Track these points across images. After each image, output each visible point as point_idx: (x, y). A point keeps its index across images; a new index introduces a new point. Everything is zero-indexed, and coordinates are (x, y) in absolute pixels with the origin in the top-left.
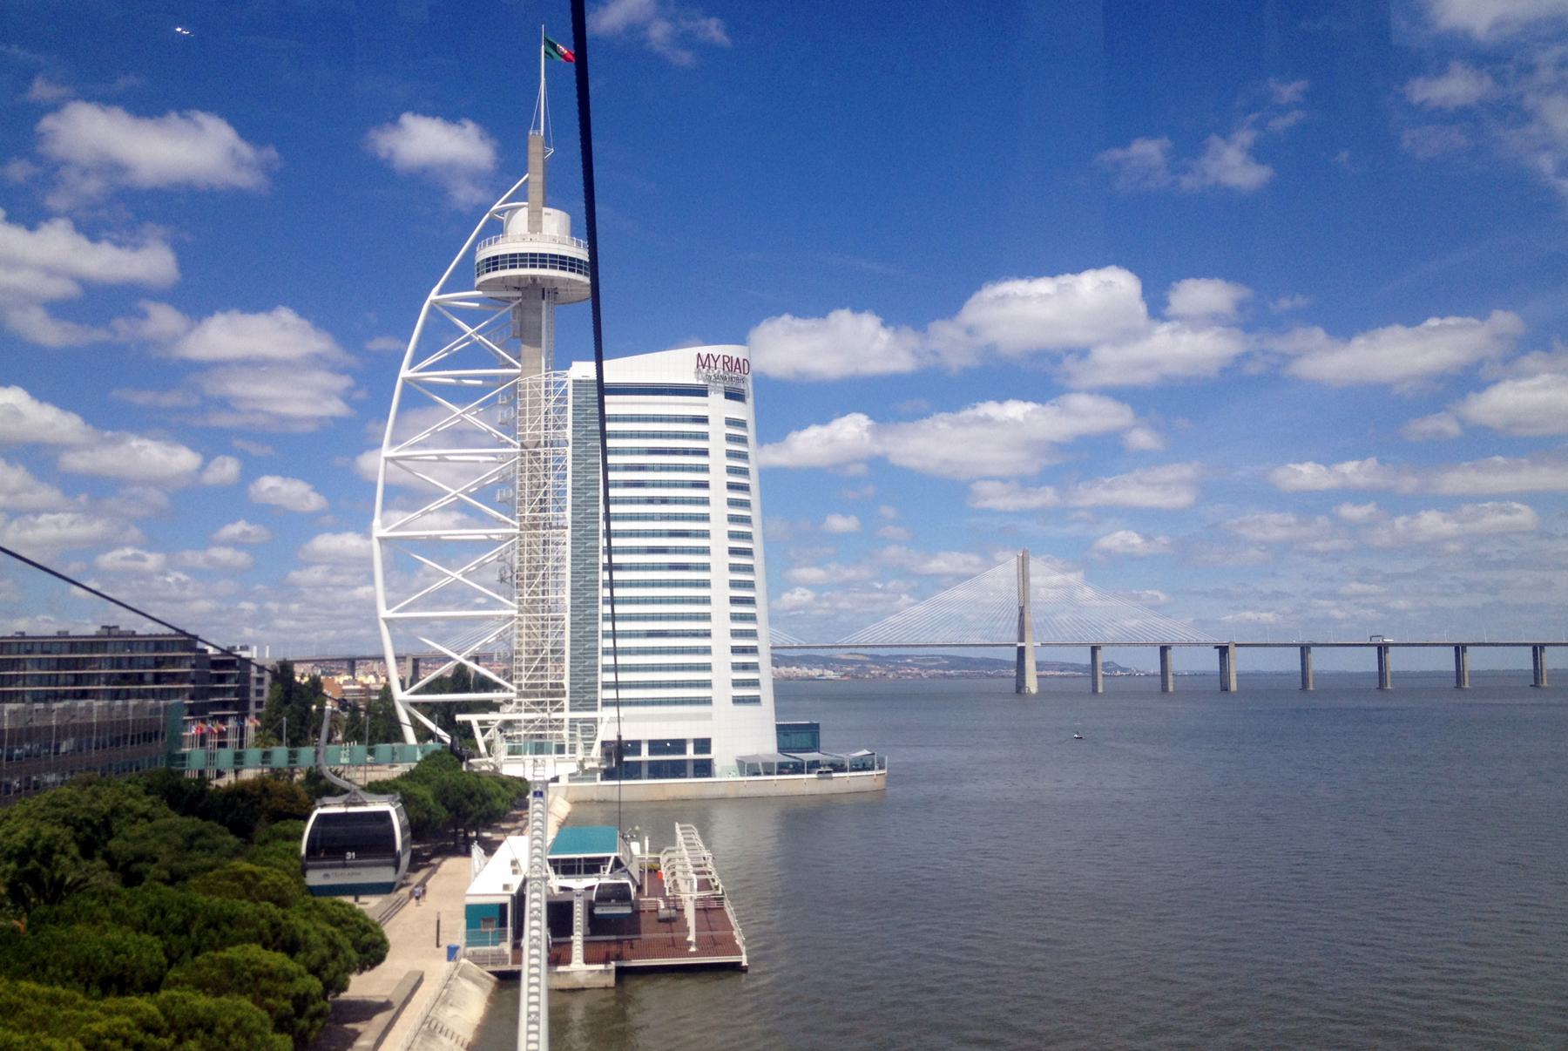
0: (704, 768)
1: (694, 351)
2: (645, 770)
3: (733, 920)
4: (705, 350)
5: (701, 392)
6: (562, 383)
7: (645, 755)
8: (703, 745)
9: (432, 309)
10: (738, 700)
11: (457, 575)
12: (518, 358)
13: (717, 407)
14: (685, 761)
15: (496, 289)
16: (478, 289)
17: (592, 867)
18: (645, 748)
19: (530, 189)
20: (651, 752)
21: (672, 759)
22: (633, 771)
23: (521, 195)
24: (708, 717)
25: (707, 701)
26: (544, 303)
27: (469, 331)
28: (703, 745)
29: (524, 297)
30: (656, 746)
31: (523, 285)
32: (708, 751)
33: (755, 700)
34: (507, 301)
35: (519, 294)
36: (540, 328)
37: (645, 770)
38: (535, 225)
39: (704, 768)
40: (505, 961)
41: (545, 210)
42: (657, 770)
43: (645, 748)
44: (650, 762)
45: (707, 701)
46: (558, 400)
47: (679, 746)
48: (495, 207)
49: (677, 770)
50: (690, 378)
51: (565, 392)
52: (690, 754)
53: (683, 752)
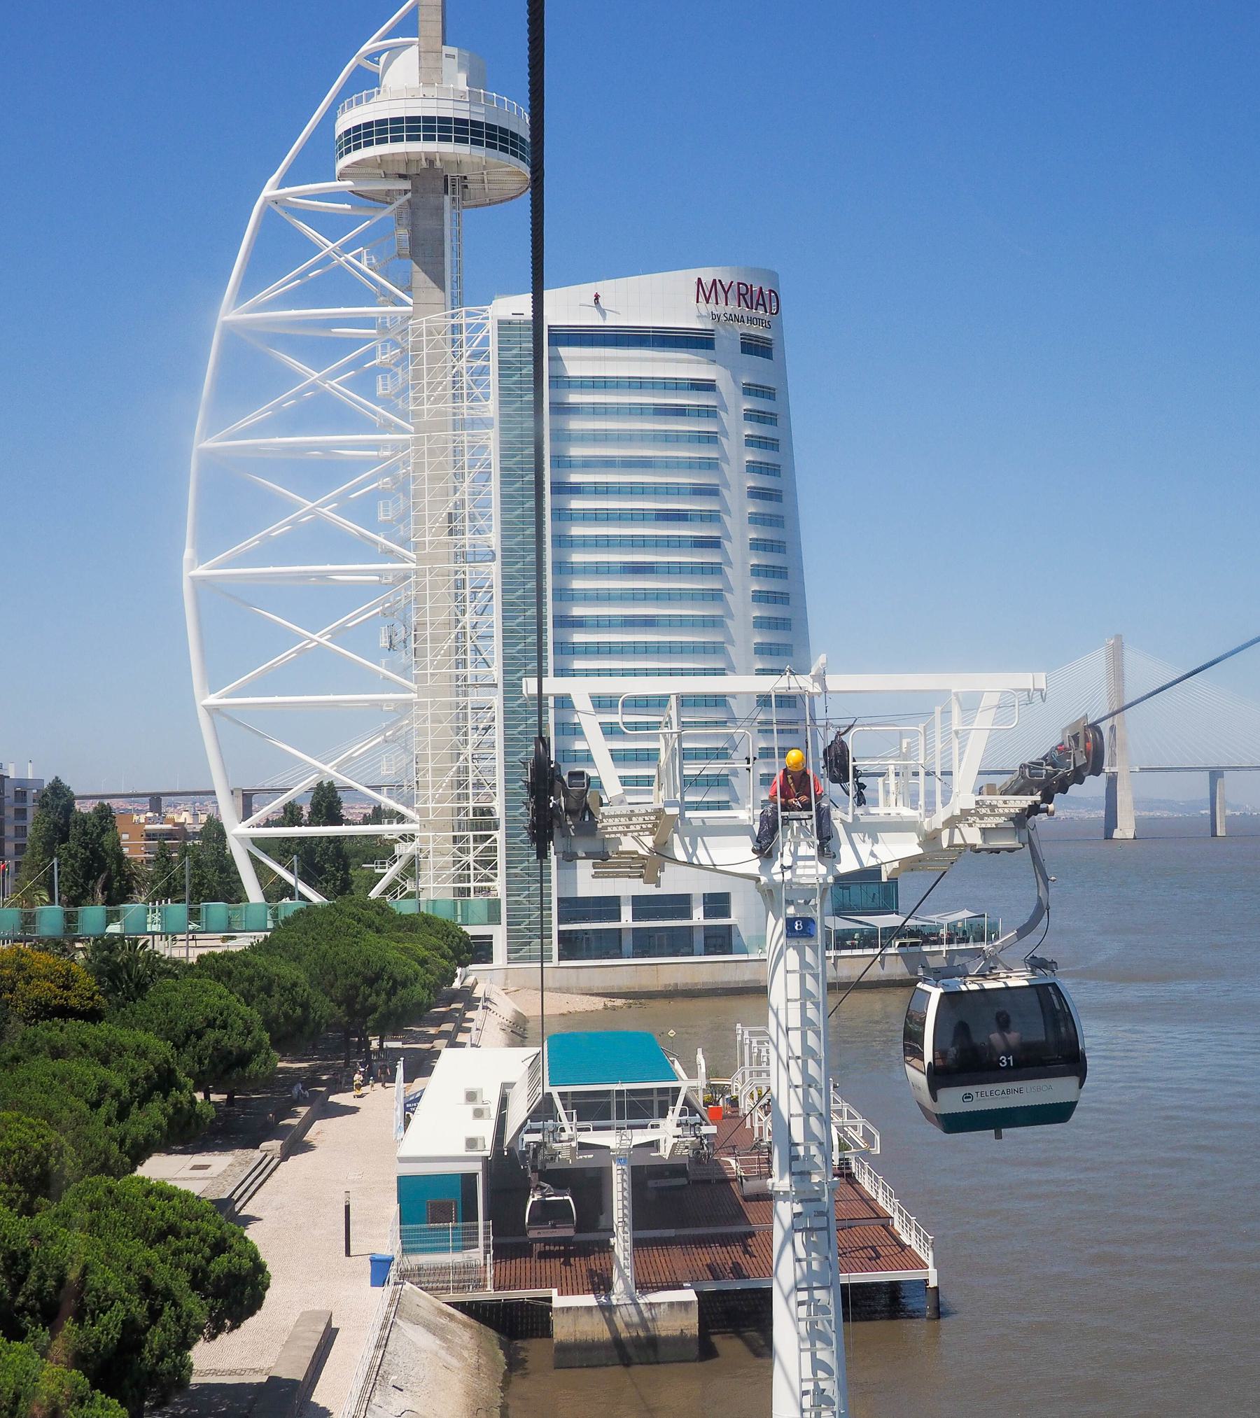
1: (693, 275)
3: (885, 1202)
6: (480, 327)
7: (627, 919)
9: (268, 214)
11: (321, 638)
12: (408, 290)
15: (371, 177)
16: (342, 176)
17: (643, 1108)
18: (627, 912)
19: (423, 15)
20: (636, 917)
22: (609, 945)
23: (409, 27)
26: (447, 199)
27: (329, 246)
28: (717, 904)
29: (415, 190)
32: (727, 914)
34: (385, 199)
35: (406, 185)
36: (442, 241)
38: (430, 73)
39: (721, 941)
40: (479, 1285)
41: (447, 49)
42: (646, 944)
43: (627, 912)
46: (475, 355)
48: (367, 47)
49: (679, 942)
50: (689, 318)
51: (485, 341)
52: (698, 917)
53: (689, 916)
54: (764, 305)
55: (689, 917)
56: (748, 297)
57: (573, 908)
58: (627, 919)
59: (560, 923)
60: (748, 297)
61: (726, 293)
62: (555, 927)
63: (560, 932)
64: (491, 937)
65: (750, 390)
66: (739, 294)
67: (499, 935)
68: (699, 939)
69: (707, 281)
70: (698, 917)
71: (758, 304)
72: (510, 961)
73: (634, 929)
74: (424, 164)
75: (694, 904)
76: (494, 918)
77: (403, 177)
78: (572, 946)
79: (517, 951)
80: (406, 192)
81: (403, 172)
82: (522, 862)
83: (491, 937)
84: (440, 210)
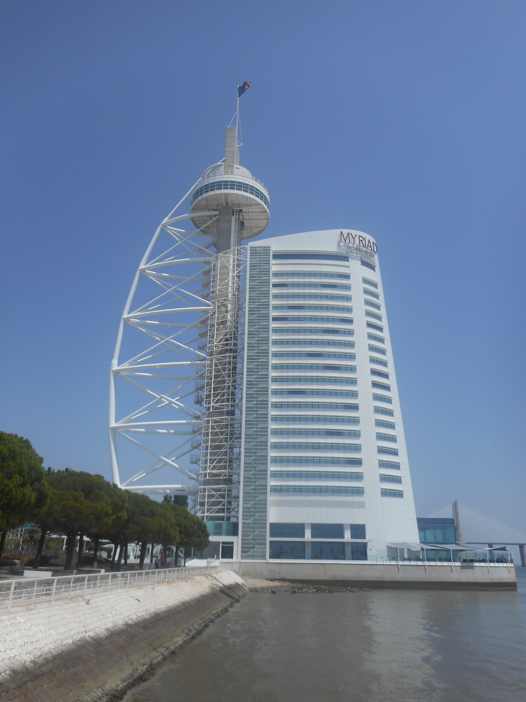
0: (360, 552)
1: (339, 231)
2: (308, 551)
4: (345, 231)
5: (345, 258)
7: (308, 536)
8: (359, 530)
10: (386, 493)
13: (356, 269)
20: (313, 536)
21: (333, 541)
22: (297, 551)
24: (362, 505)
25: (359, 491)
28: (359, 530)
29: (220, 214)
30: (319, 529)
31: (220, 208)
33: (399, 494)
35: (217, 213)
36: (230, 232)
37: (308, 551)
42: (319, 551)
44: (312, 542)
45: (359, 491)
47: (337, 530)
49: (337, 551)
52: (347, 537)
54: (371, 247)
55: (343, 537)
56: (364, 242)
57: (278, 529)
58: (308, 536)
59: (271, 535)
60: (364, 242)
61: (354, 239)
62: (269, 539)
63: (270, 542)
64: (232, 543)
65: (366, 281)
66: (360, 240)
67: (237, 541)
68: (348, 550)
69: (345, 236)
70: (347, 537)
71: (368, 246)
72: (242, 558)
73: (312, 542)
74: (224, 204)
76: (235, 533)
77: (215, 210)
78: (278, 551)
80: (217, 215)
81: (215, 208)
83: (232, 543)
84: (230, 221)
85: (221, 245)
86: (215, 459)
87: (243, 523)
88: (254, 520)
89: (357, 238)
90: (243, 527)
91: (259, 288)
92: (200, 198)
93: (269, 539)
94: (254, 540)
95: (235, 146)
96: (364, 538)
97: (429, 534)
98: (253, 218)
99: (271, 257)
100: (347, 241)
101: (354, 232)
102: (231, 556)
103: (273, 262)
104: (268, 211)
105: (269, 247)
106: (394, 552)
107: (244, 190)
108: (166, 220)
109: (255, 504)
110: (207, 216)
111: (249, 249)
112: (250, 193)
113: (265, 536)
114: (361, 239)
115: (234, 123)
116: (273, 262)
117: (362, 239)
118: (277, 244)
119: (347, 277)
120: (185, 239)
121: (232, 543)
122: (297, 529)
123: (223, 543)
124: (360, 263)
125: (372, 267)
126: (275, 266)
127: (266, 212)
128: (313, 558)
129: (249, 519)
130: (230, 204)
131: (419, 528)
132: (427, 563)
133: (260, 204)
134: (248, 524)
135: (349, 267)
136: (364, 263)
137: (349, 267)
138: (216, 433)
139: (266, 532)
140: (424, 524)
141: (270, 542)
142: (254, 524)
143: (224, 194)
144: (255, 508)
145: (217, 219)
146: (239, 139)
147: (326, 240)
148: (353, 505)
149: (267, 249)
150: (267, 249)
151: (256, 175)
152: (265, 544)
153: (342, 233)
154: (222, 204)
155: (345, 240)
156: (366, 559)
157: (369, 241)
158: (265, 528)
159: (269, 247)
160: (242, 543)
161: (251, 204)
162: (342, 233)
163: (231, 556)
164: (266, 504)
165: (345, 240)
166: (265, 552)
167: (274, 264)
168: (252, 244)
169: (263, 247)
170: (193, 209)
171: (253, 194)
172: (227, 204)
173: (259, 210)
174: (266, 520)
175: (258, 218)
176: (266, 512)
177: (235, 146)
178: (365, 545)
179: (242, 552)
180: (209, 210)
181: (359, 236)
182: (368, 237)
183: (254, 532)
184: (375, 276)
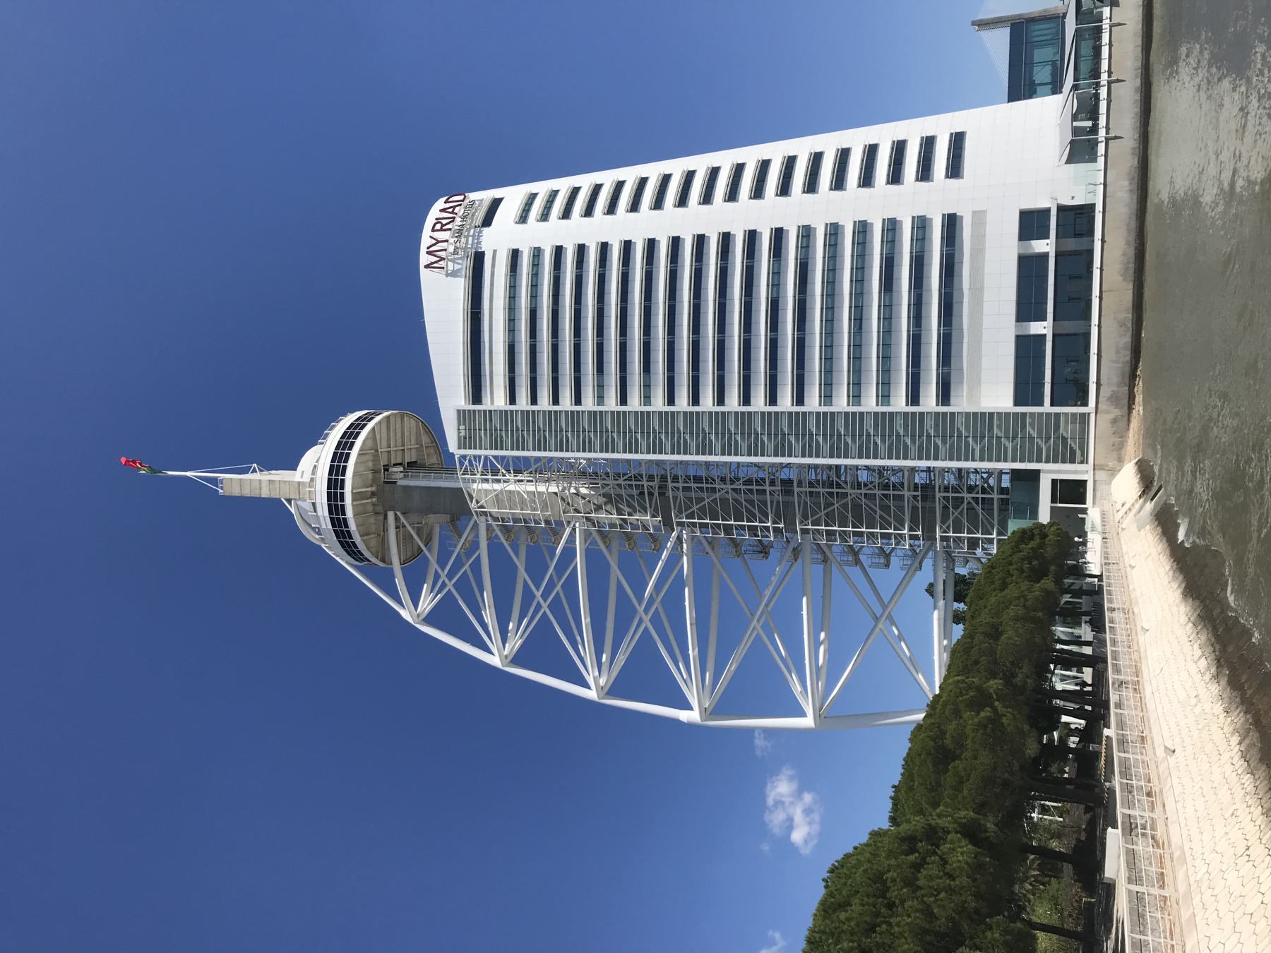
0: (1077, 220)
1: (424, 274)
4: (424, 259)
5: (479, 258)
7: (1042, 328)
8: (1032, 223)
10: (955, 169)
13: (499, 239)
14: (1058, 255)
22: (1072, 349)
24: (979, 216)
25: (951, 222)
28: (1032, 223)
29: (393, 508)
30: (1028, 307)
33: (958, 140)
35: (391, 515)
42: (1074, 303)
43: (1037, 328)
45: (951, 222)
47: (1030, 268)
49: (1076, 267)
52: (1045, 246)
54: (454, 207)
55: (1045, 256)
56: (444, 222)
57: (1026, 390)
58: (1042, 328)
59: (1041, 404)
60: (444, 222)
61: (438, 242)
62: (1047, 408)
63: (1052, 405)
66: (441, 230)
67: (1050, 472)
70: (1045, 246)
72: (1084, 461)
73: (1054, 320)
75: (1030, 251)
76: (1035, 475)
77: (386, 517)
78: (1072, 388)
79: (1073, 452)
81: (381, 518)
82: (967, 444)
83: (1054, 482)
84: (406, 488)
85: (456, 507)
86: (881, 517)
87: (1014, 460)
88: (1007, 437)
89: (437, 235)
90: (1022, 461)
91: (539, 430)
92: (362, 547)
93: (1047, 408)
94: (1048, 439)
95: (259, 482)
96: (1048, 211)
97: (1042, 74)
98: (399, 441)
99: (477, 407)
100: (443, 254)
101: (426, 241)
102: (1083, 483)
103: (486, 405)
104: (386, 414)
105: (459, 411)
106: (1081, 149)
107: (346, 461)
108: (405, 614)
109: (974, 437)
110: (397, 534)
111: (463, 452)
112: (350, 448)
113: (1040, 415)
114: (438, 227)
115: (214, 481)
116: (486, 405)
117: (440, 225)
118: (451, 394)
119: (515, 254)
120: (443, 577)
121: (1054, 482)
122: (1027, 349)
123: (1053, 500)
124: (485, 230)
125: (496, 203)
126: (496, 399)
127: (388, 417)
128: (1088, 317)
129: (1006, 449)
130: (374, 489)
131: (1030, 97)
132: (1104, 77)
133: (373, 429)
134: (1015, 449)
135: (495, 251)
136: (487, 221)
137: (495, 251)
138: (827, 515)
139: (1032, 414)
140: (1021, 86)
141: (1052, 405)
142: (1014, 438)
143: (353, 500)
144: (983, 437)
145: (403, 514)
146: (245, 471)
147: (442, 298)
148: (979, 238)
149: (462, 415)
150: (462, 415)
151: (315, 437)
152: (1057, 415)
153: (427, 266)
154: (374, 505)
155: (443, 259)
156: (1092, 207)
157: (443, 210)
158: (1024, 415)
159: (459, 411)
160: (1055, 461)
161: (371, 449)
162: (427, 266)
163: (1083, 483)
164: (975, 414)
165: (443, 259)
166: (1074, 415)
167: (492, 403)
168: (452, 446)
169: (459, 424)
170: (383, 561)
171: (353, 443)
172: (373, 494)
173: (384, 430)
174: (1007, 414)
175: (399, 435)
176: (991, 414)
177: (259, 482)
178: (1062, 209)
179: (1073, 461)
180: (385, 530)
181: (433, 230)
182: (435, 213)
183: (1031, 438)
184: (513, 196)
